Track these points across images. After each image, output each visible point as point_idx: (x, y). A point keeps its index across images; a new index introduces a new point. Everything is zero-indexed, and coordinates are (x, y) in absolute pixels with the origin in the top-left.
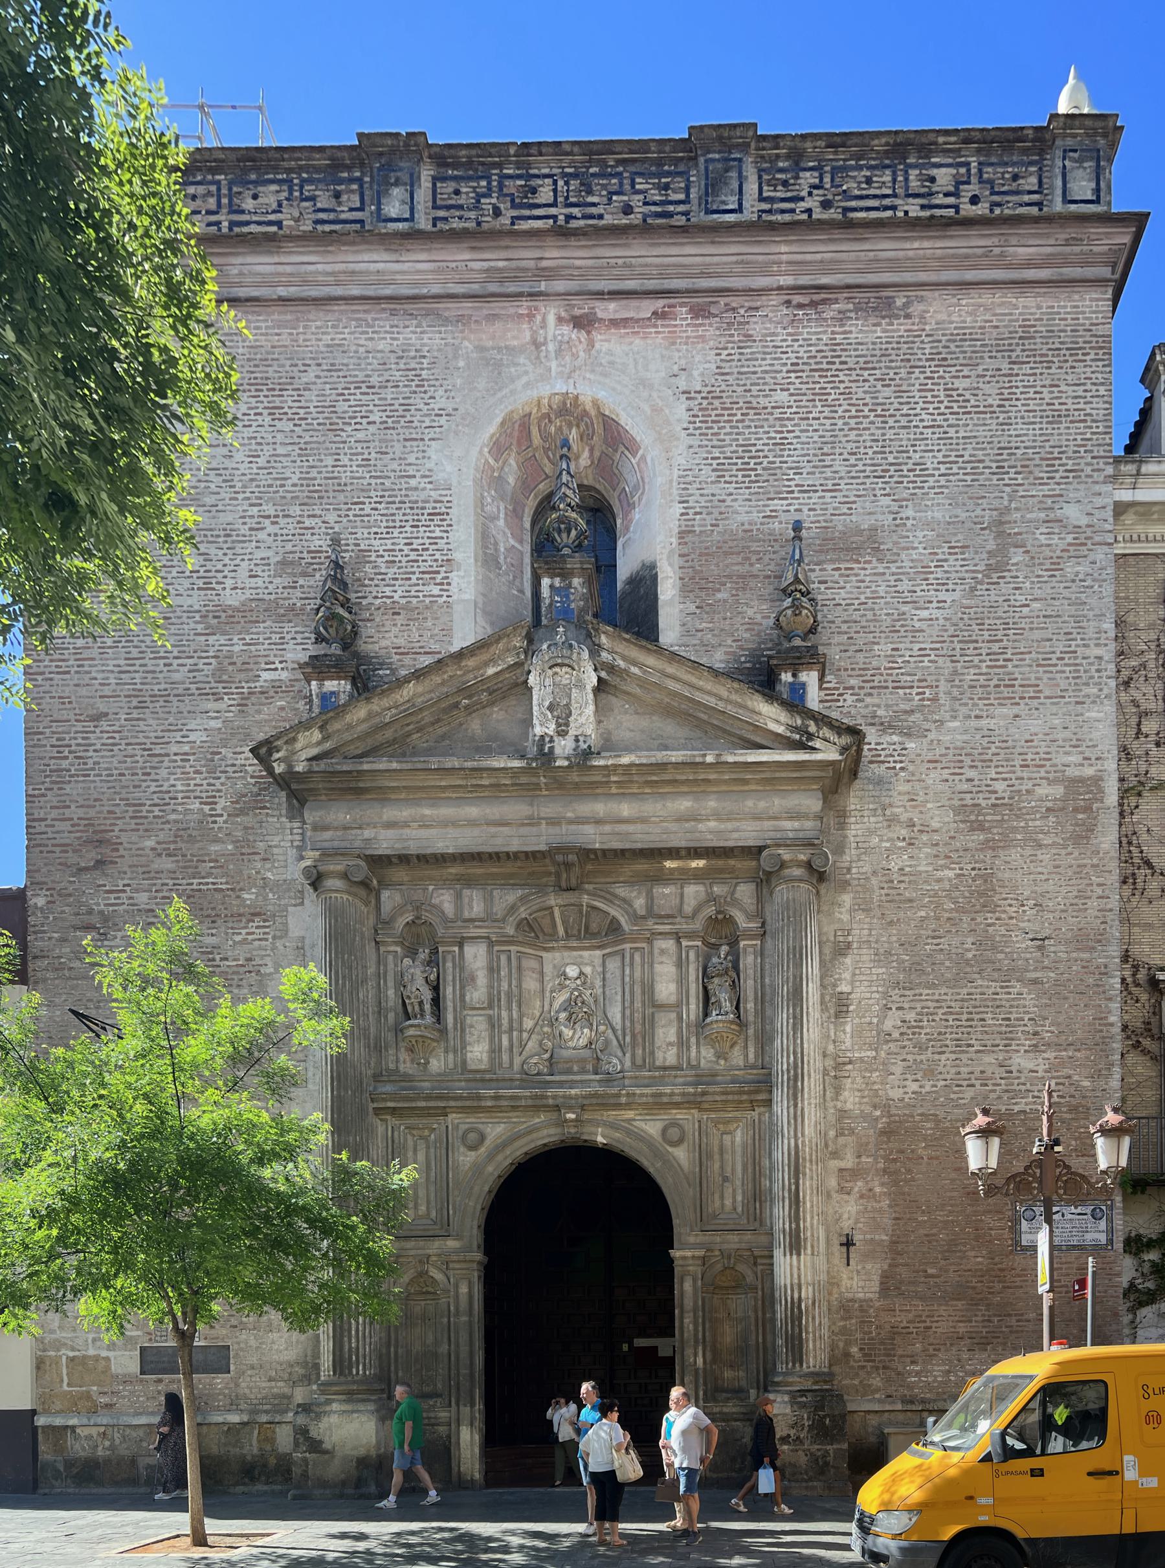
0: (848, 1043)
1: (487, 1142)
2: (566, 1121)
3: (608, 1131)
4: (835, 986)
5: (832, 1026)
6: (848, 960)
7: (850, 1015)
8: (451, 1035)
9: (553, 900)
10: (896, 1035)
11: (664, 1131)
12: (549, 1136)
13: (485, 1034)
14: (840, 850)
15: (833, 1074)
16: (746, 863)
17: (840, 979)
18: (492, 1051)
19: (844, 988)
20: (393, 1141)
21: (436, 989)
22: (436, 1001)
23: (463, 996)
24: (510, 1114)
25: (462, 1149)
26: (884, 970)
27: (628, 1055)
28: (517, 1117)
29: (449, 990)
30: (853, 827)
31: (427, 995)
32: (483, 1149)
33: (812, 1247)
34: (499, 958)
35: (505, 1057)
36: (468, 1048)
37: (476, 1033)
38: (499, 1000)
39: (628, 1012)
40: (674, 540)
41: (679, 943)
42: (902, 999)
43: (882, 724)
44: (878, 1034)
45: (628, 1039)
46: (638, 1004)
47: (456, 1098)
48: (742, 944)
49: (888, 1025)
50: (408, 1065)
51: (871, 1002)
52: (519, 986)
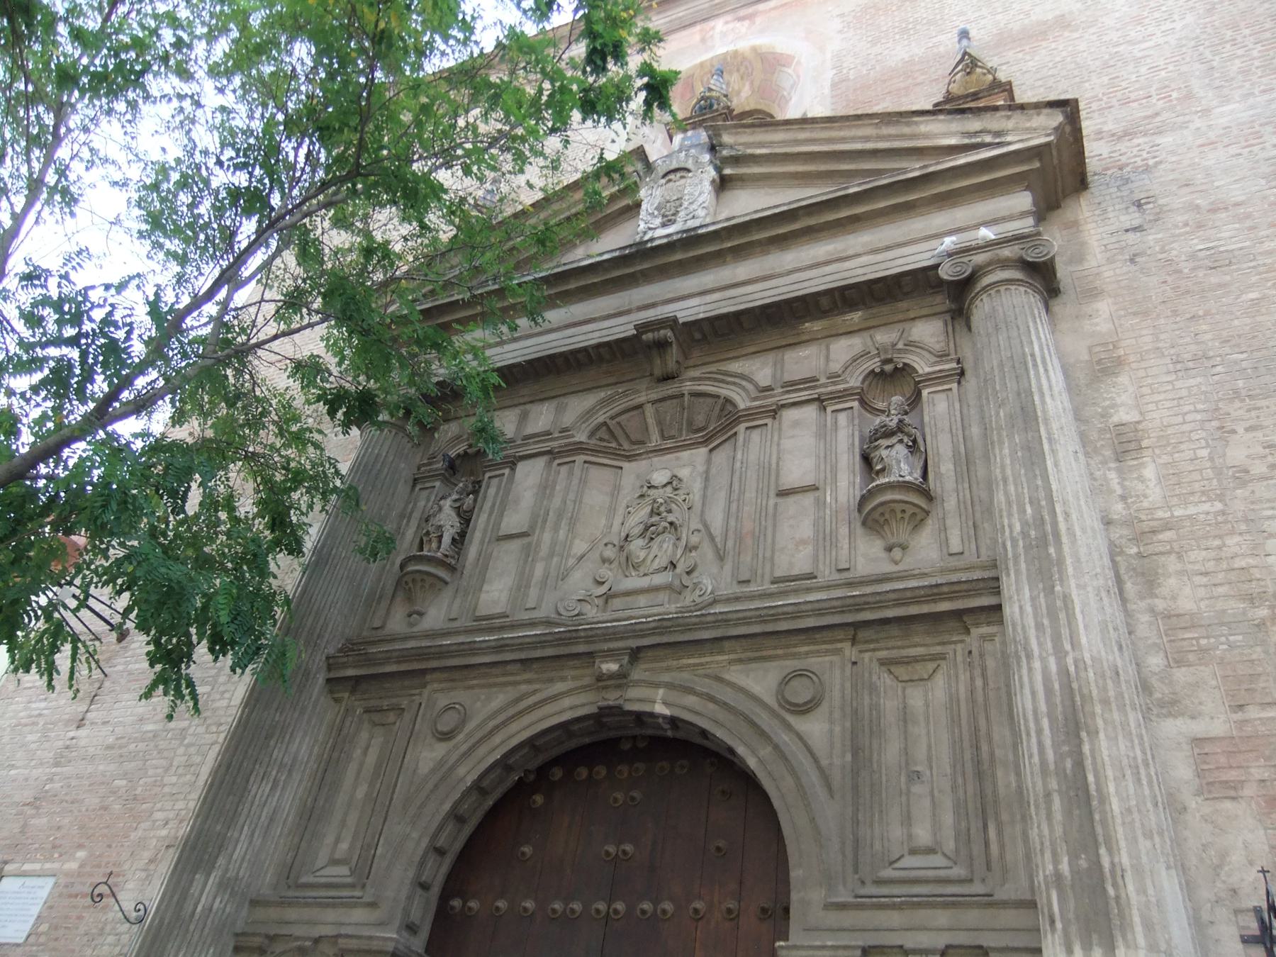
0: (1154, 494)
3: (675, 696)
4: (1105, 415)
5: (1113, 475)
6: (1123, 379)
7: (1145, 453)
10: (1259, 468)
14: (1079, 257)
15: (1134, 550)
17: (1113, 406)
19: (1124, 415)
24: (518, 678)
26: (1199, 380)
27: (728, 567)
28: (529, 682)
30: (1092, 232)
32: (461, 737)
33: (1148, 927)
35: (533, 593)
39: (734, 506)
40: (827, 91)
42: (1254, 413)
43: (1113, 135)
44: (1218, 472)
45: (730, 544)
48: (925, 393)
49: (1237, 454)
51: (1186, 427)
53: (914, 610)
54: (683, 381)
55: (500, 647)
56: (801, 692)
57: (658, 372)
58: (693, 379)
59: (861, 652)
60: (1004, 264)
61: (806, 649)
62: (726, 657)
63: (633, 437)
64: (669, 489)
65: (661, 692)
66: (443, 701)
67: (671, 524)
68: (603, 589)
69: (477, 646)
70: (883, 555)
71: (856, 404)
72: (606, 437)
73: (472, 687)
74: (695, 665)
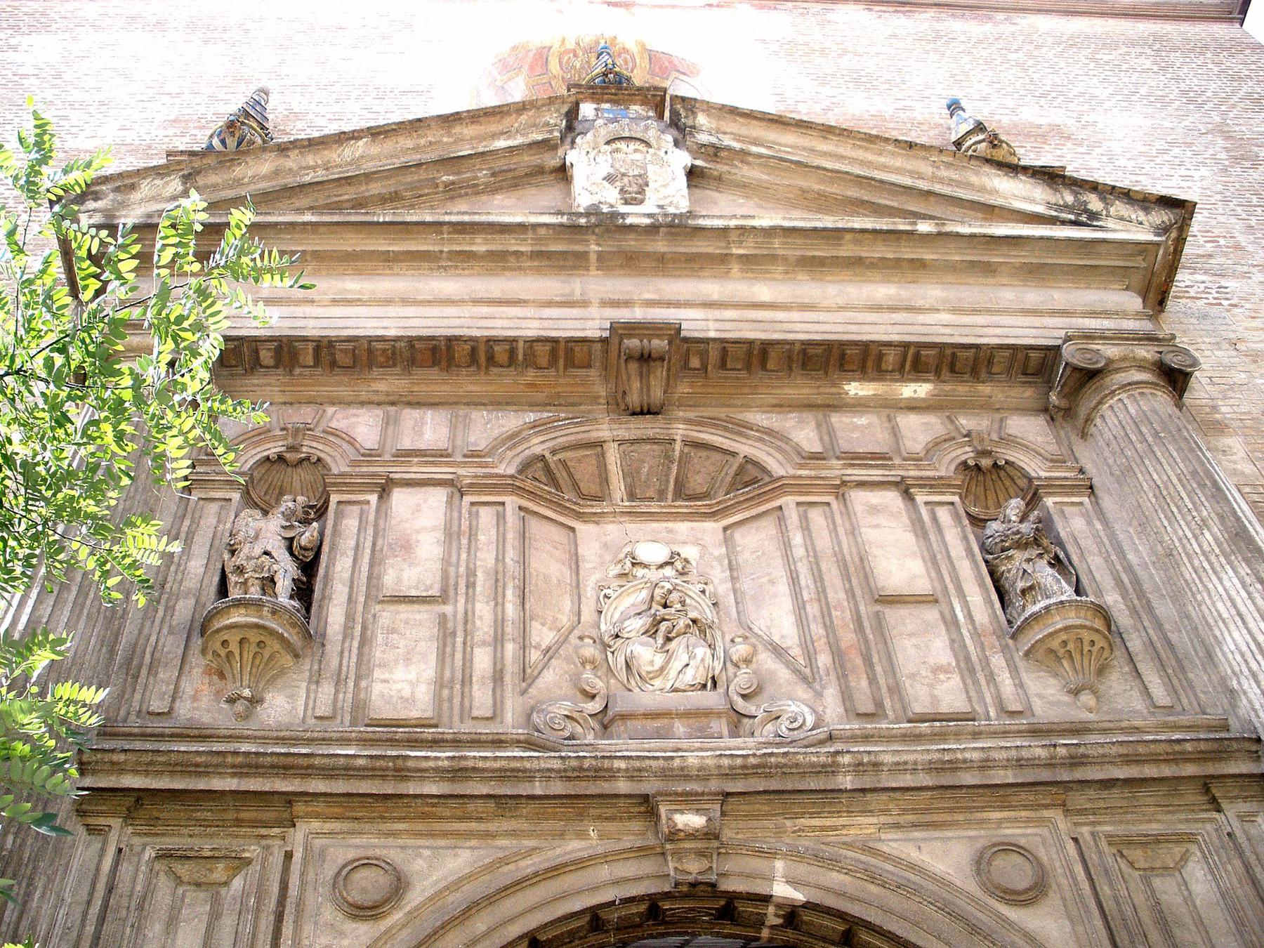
1: (414, 898)
2: (674, 835)
8: (332, 649)
9: (604, 430)
11: (981, 863)
12: (617, 882)
13: (430, 650)
16: (1013, 392)
18: (440, 683)
20: (110, 890)
21: (309, 565)
22: (304, 592)
23: (373, 580)
24: (492, 826)
25: (329, 913)
28: (513, 834)
29: (342, 566)
31: (286, 572)
32: (397, 916)
34: (474, 516)
36: (377, 674)
37: (402, 643)
38: (470, 585)
41: (907, 495)
46: (836, 593)
47: (329, 773)
48: (1049, 501)
50: (205, 702)
52: (523, 561)
53: (1150, 771)
54: (671, 420)
55: (458, 773)
56: (1016, 873)
57: (634, 399)
58: (688, 421)
59: (1075, 824)
60: (1141, 366)
61: (996, 815)
62: (874, 820)
63: (584, 487)
64: (668, 571)
65: (779, 865)
66: (341, 853)
67: (694, 621)
68: (595, 706)
69: (410, 764)
70: (1066, 698)
71: (956, 499)
72: (544, 479)
73: (394, 834)
74: (823, 829)
